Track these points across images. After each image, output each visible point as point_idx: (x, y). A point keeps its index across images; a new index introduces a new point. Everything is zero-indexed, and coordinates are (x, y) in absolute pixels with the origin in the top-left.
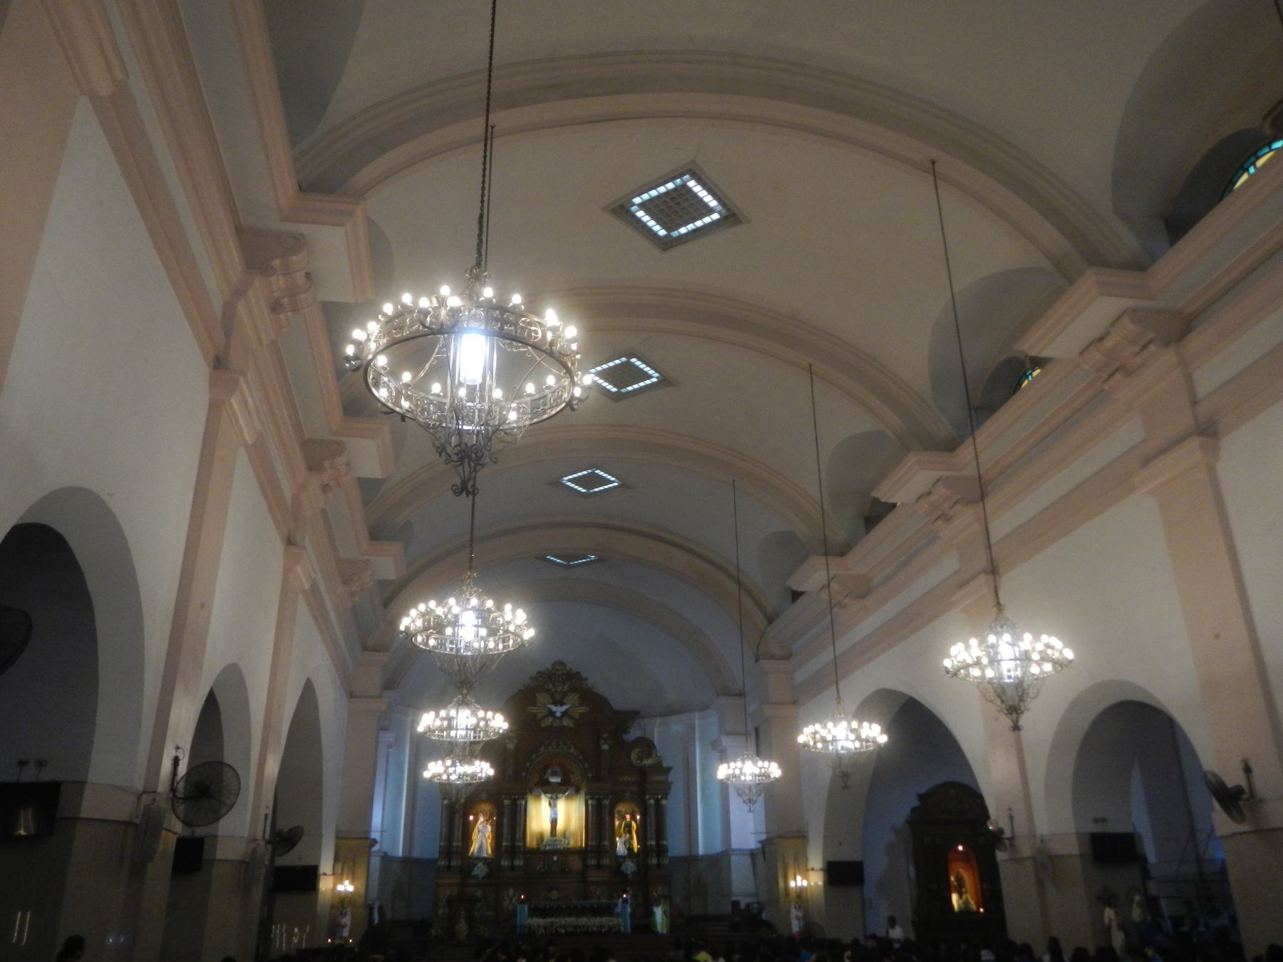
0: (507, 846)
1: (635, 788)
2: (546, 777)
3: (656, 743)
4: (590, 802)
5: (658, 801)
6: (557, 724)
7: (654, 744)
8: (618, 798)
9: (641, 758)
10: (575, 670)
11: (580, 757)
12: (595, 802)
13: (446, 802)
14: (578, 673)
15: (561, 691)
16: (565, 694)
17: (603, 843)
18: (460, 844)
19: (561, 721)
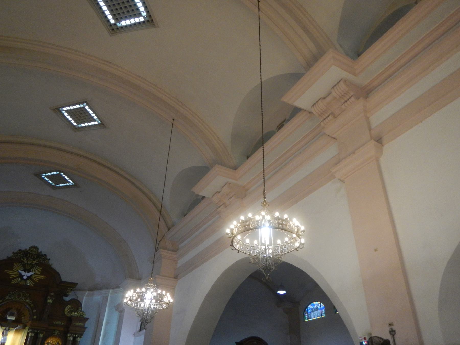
1: (62, 329)
2: (5, 316)
3: (83, 305)
4: (30, 334)
5: (75, 338)
6: (22, 283)
8: (50, 334)
9: (71, 311)
10: (43, 253)
11: (32, 305)
12: (33, 335)
14: (45, 255)
15: (31, 264)
16: (33, 266)
19: (26, 282)
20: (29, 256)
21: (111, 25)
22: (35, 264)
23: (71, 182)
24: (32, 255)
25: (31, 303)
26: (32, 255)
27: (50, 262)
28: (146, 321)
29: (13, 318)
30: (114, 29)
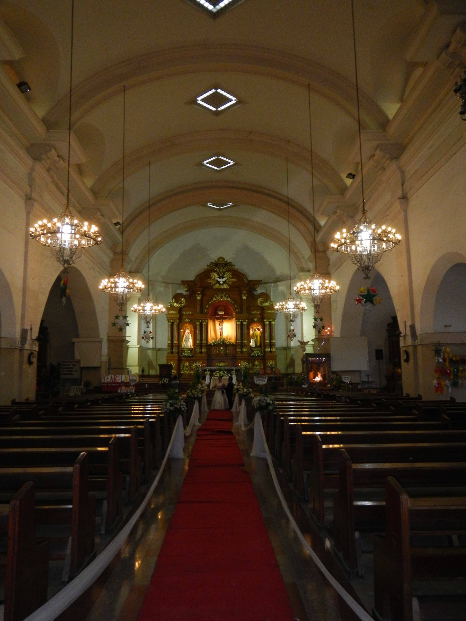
0: (199, 343)
1: (259, 316)
4: (237, 323)
5: (270, 322)
6: (221, 287)
8: (251, 322)
9: (262, 303)
10: (229, 261)
11: (233, 302)
12: (240, 323)
13: (170, 323)
14: (231, 262)
15: (223, 271)
16: (224, 273)
17: (244, 342)
18: (177, 342)
19: (223, 286)
20: (219, 266)
21: (214, 111)
23: (231, 204)
24: (221, 265)
26: (221, 265)
27: (236, 267)
29: (223, 313)
30: (217, 113)
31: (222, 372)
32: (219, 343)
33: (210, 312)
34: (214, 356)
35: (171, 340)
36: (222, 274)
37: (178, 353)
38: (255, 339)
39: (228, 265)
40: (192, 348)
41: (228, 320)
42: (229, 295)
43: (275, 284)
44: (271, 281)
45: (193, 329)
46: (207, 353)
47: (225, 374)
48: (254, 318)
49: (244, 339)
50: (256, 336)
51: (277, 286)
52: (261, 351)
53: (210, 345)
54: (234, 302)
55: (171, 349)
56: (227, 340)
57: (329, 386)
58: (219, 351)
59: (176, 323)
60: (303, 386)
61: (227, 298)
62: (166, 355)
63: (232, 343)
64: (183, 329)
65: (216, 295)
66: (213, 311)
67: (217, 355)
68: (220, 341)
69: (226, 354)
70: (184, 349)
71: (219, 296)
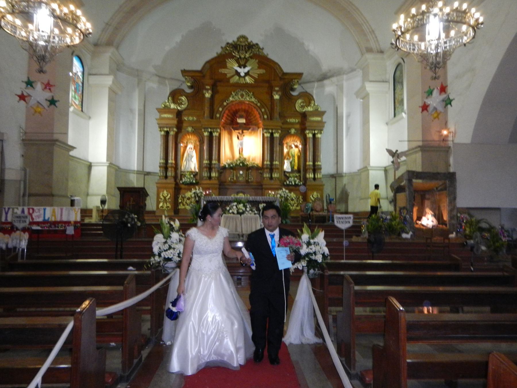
0: (207, 164)
3: (314, 97)
4: (266, 135)
6: (242, 81)
7: (313, 97)
8: (286, 134)
9: (303, 107)
10: (255, 42)
11: (259, 104)
12: (269, 135)
13: (163, 133)
14: (257, 44)
15: (245, 58)
16: (247, 60)
18: (174, 162)
22: (248, 57)
25: (256, 102)
27: (265, 52)
28: (437, 65)
31: (242, 205)
32: (236, 165)
33: (224, 118)
34: (230, 184)
35: (164, 158)
36: (244, 61)
37: (175, 177)
38: (291, 159)
39: (253, 48)
40: (197, 170)
41: (250, 133)
42: (253, 93)
43: (320, 83)
44: (313, 80)
45: (198, 143)
46: (219, 178)
47: (248, 209)
48: (290, 129)
49: (275, 158)
50: (292, 155)
51: (323, 86)
52: (299, 177)
53: (224, 168)
54: (261, 104)
55: (164, 172)
56: (249, 161)
57: (453, 236)
58: (237, 177)
59: (172, 133)
60: (404, 236)
61: (251, 97)
62: (156, 181)
63: (257, 165)
64: (183, 142)
65: (234, 92)
66: (230, 119)
67: (234, 183)
68: (239, 162)
69: (247, 182)
70: (184, 172)
71: (238, 94)
